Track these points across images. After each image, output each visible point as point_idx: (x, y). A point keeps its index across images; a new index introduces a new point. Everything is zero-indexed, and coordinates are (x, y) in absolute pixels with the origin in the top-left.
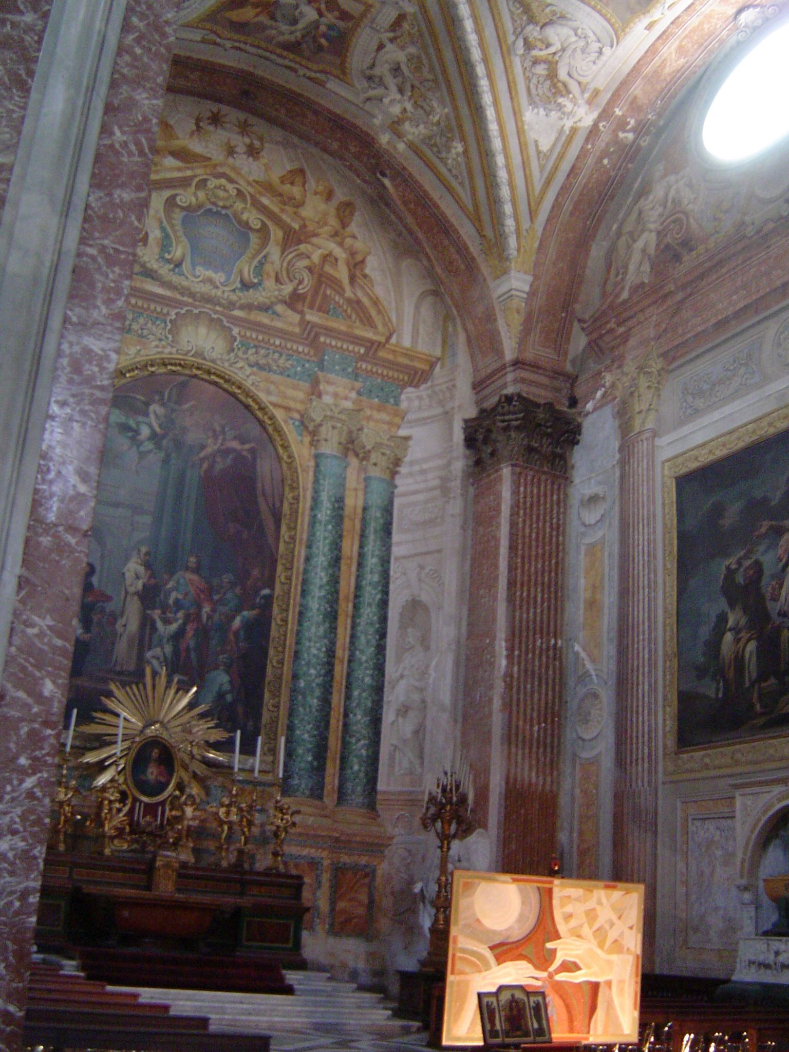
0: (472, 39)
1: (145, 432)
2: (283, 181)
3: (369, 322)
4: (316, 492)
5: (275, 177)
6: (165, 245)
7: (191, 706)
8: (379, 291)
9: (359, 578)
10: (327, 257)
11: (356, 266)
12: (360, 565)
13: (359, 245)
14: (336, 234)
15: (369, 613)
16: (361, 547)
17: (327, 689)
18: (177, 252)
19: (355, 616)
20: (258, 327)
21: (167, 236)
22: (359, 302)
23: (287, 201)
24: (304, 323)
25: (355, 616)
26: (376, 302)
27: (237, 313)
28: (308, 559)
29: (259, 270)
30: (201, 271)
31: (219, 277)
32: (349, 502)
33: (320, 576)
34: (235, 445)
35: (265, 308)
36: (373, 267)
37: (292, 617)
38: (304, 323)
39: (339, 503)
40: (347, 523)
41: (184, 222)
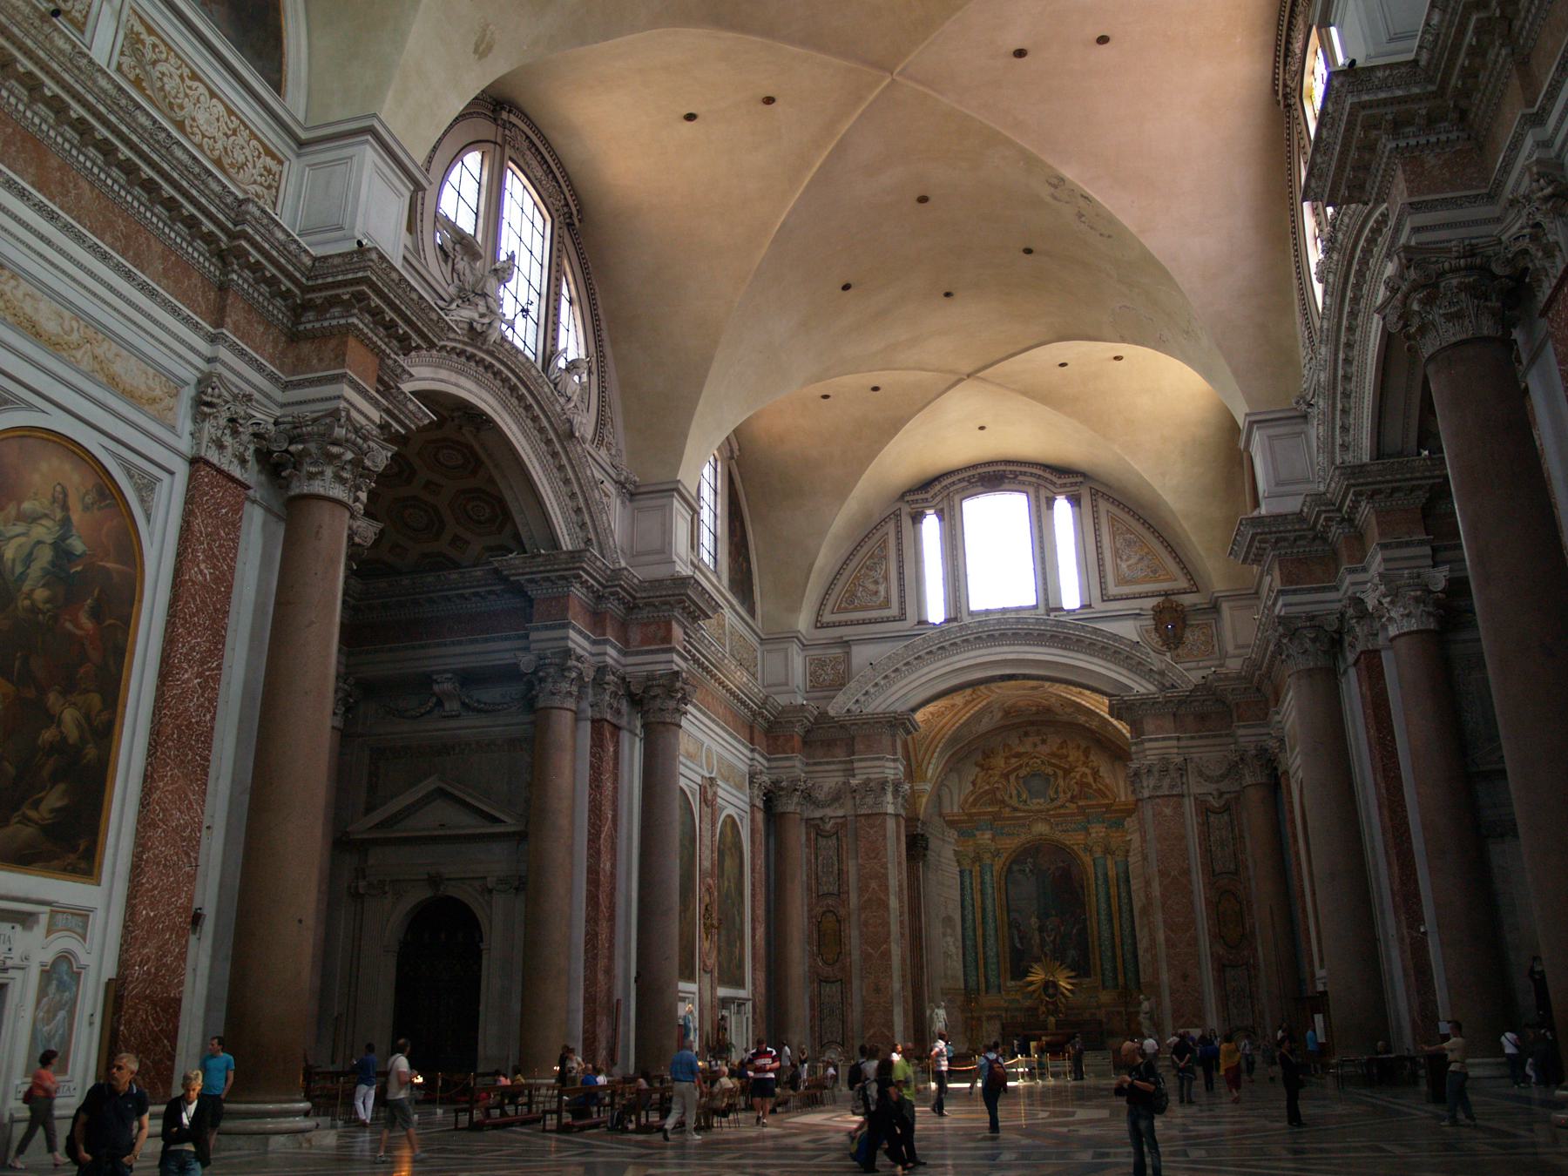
0: (1088, 705)
1: (1027, 870)
2: (1058, 749)
3: (1104, 795)
4: (1096, 873)
5: (1055, 749)
6: (1019, 796)
7: (1060, 965)
8: (1107, 781)
9: (1119, 902)
10: (1084, 775)
11: (1095, 773)
12: (1119, 897)
13: (1095, 764)
14: (1084, 763)
15: (1126, 915)
16: (1118, 889)
17: (1113, 948)
18: (1024, 797)
19: (1120, 917)
20: (1059, 815)
21: (1019, 792)
22: (1100, 789)
23: (1061, 757)
24: (1078, 807)
25: (1120, 917)
26: (1106, 786)
27: (1052, 813)
28: (1097, 901)
29: (1056, 792)
30: (1035, 801)
31: (1042, 800)
32: (1110, 873)
33: (1103, 906)
34: (1062, 864)
35: (1062, 806)
36: (1103, 771)
37: (1095, 925)
38: (1078, 807)
39: (1106, 874)
40: (1111, 883)
41: (1024, 783)
